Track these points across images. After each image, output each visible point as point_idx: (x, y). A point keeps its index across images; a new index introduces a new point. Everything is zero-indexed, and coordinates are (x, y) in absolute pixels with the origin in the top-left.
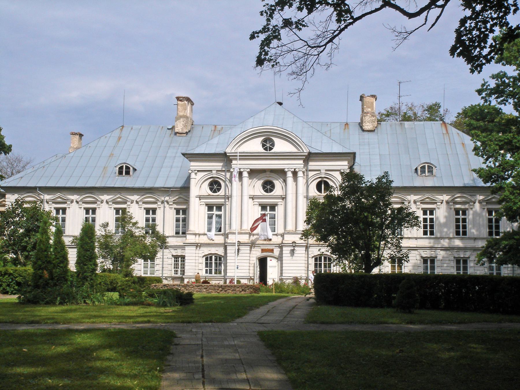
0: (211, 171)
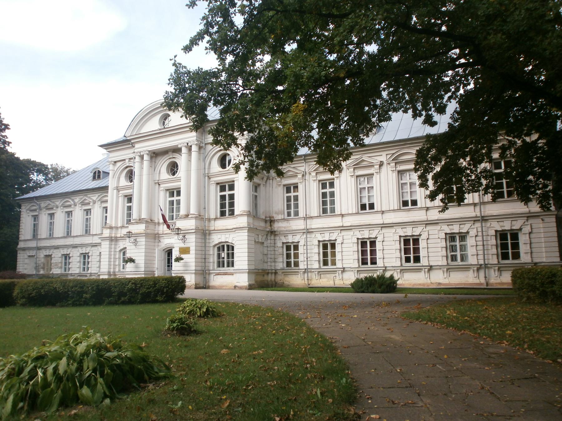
0: (124, 160)
